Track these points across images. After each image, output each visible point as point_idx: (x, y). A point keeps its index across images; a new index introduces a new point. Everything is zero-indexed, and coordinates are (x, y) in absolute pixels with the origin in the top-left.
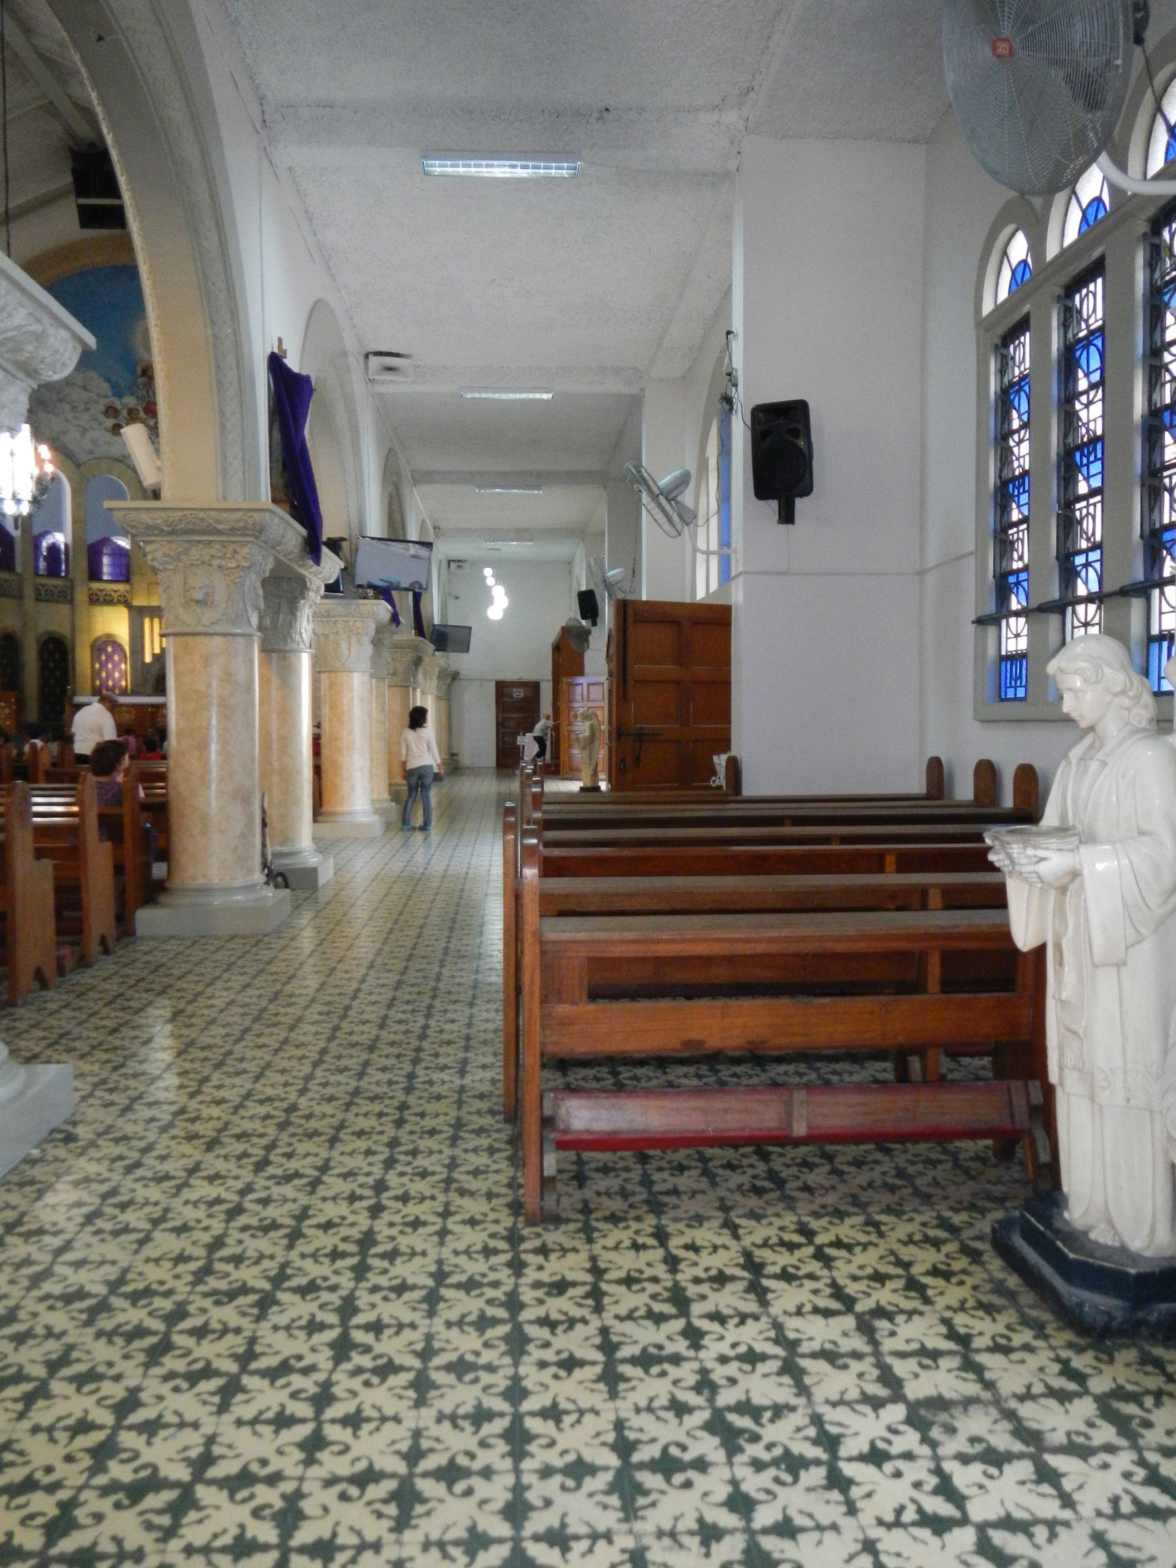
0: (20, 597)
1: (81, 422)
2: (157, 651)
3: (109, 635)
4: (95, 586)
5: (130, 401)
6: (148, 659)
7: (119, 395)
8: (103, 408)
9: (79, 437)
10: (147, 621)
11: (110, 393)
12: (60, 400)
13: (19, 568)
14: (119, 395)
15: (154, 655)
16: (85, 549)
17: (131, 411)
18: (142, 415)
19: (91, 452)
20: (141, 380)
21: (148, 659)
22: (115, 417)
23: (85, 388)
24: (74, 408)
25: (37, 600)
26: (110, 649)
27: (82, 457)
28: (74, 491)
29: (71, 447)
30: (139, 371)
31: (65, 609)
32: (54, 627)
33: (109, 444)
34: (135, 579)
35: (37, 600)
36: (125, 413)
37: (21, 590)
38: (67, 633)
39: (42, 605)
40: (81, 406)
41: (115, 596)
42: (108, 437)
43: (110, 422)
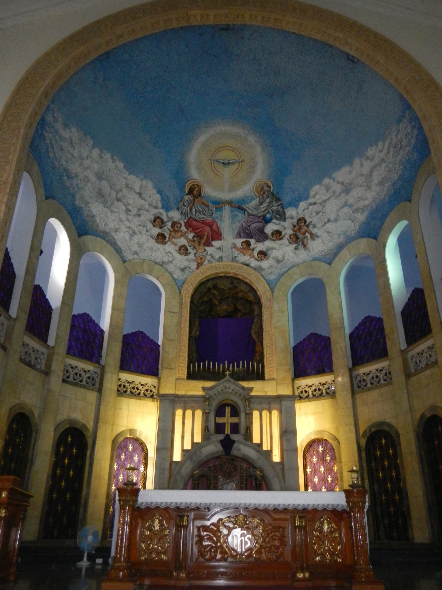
0: (47, 373)
1: (132, 225)
2: (188, 446)
3: (131, 431)
4: (126, 377)
5: (175, 215)
6: (177, 456)
7: (167, 209)
8: (152, 218)
9: (128, 237)
10: (179, 413)
11: (160, 205)
12: (119, 200)
13: (51, 341)
14: (167, 209)
15: (184, 452)
16: (121, 338)
17: (174, 224)
18: (183, 228)
19: (136, 253)
20: (187, 198)
21: (177, 456)
22: (161, 228)
23: (140, 194)
24: (128, 210)
25: (64, 381)
26: (130, 448)
27: (128, 255)
28: (117, 282)
29: (120, 244)
30: (187, 190)
31: (92, 396)
32: (77, 416)
33: (151, 249)
34: (163, 373)
35: (64, 381)
36: (169, 224)
37: (49, 365)
38: (90, 426)
39: (69, 387)
40: (134, 211)
41: (142, 389)
42: (152, 243)
43: (156, 231)
